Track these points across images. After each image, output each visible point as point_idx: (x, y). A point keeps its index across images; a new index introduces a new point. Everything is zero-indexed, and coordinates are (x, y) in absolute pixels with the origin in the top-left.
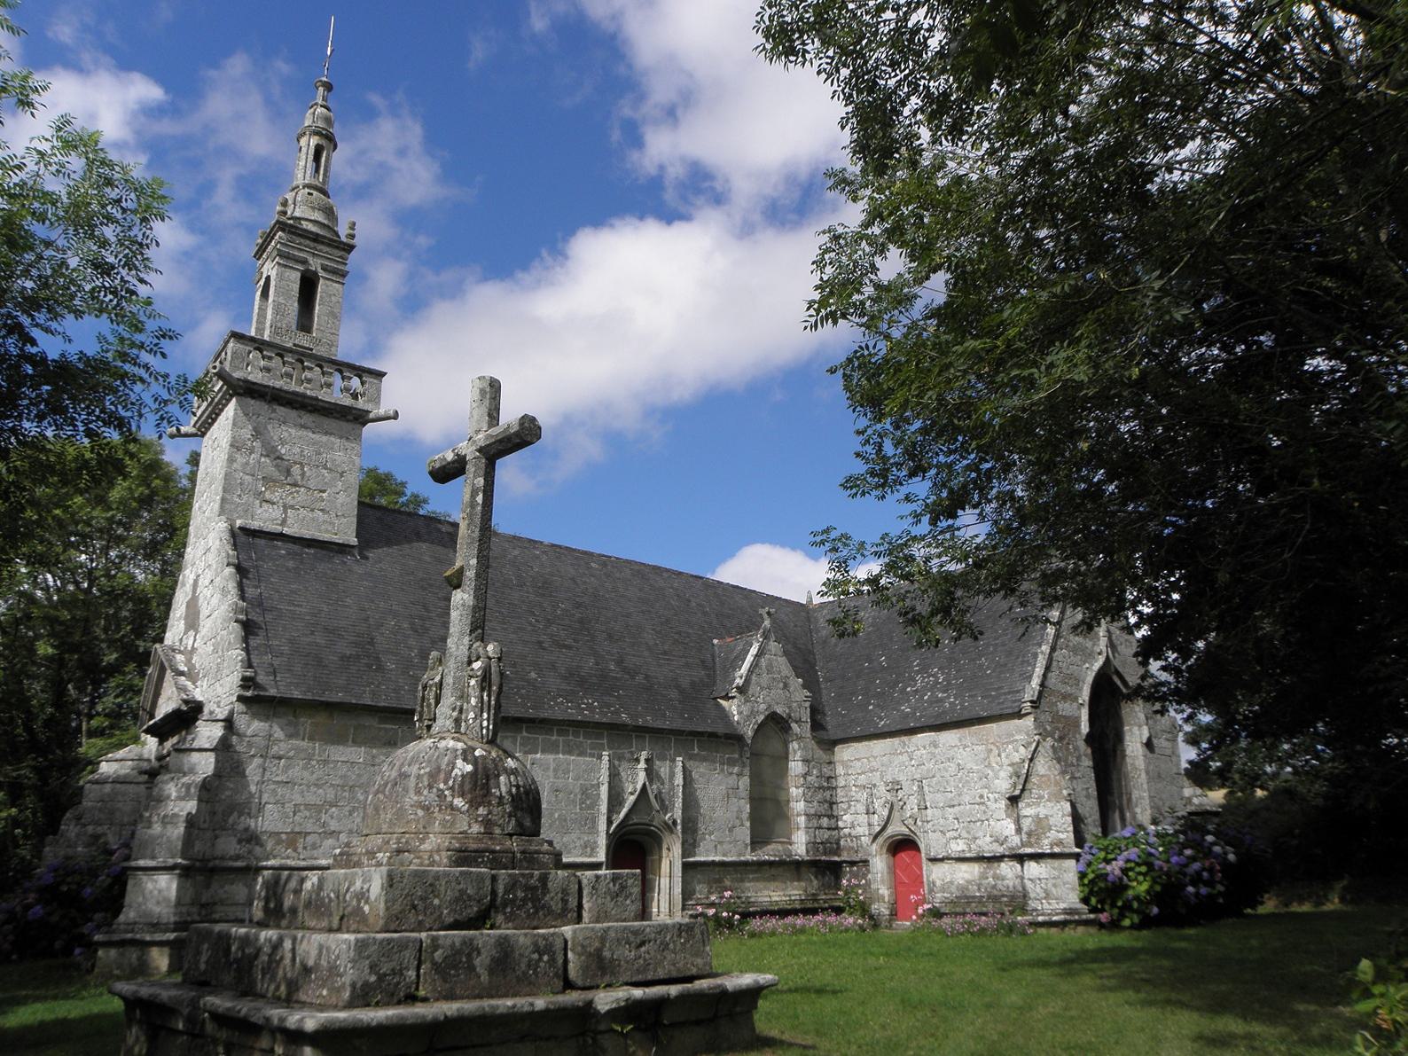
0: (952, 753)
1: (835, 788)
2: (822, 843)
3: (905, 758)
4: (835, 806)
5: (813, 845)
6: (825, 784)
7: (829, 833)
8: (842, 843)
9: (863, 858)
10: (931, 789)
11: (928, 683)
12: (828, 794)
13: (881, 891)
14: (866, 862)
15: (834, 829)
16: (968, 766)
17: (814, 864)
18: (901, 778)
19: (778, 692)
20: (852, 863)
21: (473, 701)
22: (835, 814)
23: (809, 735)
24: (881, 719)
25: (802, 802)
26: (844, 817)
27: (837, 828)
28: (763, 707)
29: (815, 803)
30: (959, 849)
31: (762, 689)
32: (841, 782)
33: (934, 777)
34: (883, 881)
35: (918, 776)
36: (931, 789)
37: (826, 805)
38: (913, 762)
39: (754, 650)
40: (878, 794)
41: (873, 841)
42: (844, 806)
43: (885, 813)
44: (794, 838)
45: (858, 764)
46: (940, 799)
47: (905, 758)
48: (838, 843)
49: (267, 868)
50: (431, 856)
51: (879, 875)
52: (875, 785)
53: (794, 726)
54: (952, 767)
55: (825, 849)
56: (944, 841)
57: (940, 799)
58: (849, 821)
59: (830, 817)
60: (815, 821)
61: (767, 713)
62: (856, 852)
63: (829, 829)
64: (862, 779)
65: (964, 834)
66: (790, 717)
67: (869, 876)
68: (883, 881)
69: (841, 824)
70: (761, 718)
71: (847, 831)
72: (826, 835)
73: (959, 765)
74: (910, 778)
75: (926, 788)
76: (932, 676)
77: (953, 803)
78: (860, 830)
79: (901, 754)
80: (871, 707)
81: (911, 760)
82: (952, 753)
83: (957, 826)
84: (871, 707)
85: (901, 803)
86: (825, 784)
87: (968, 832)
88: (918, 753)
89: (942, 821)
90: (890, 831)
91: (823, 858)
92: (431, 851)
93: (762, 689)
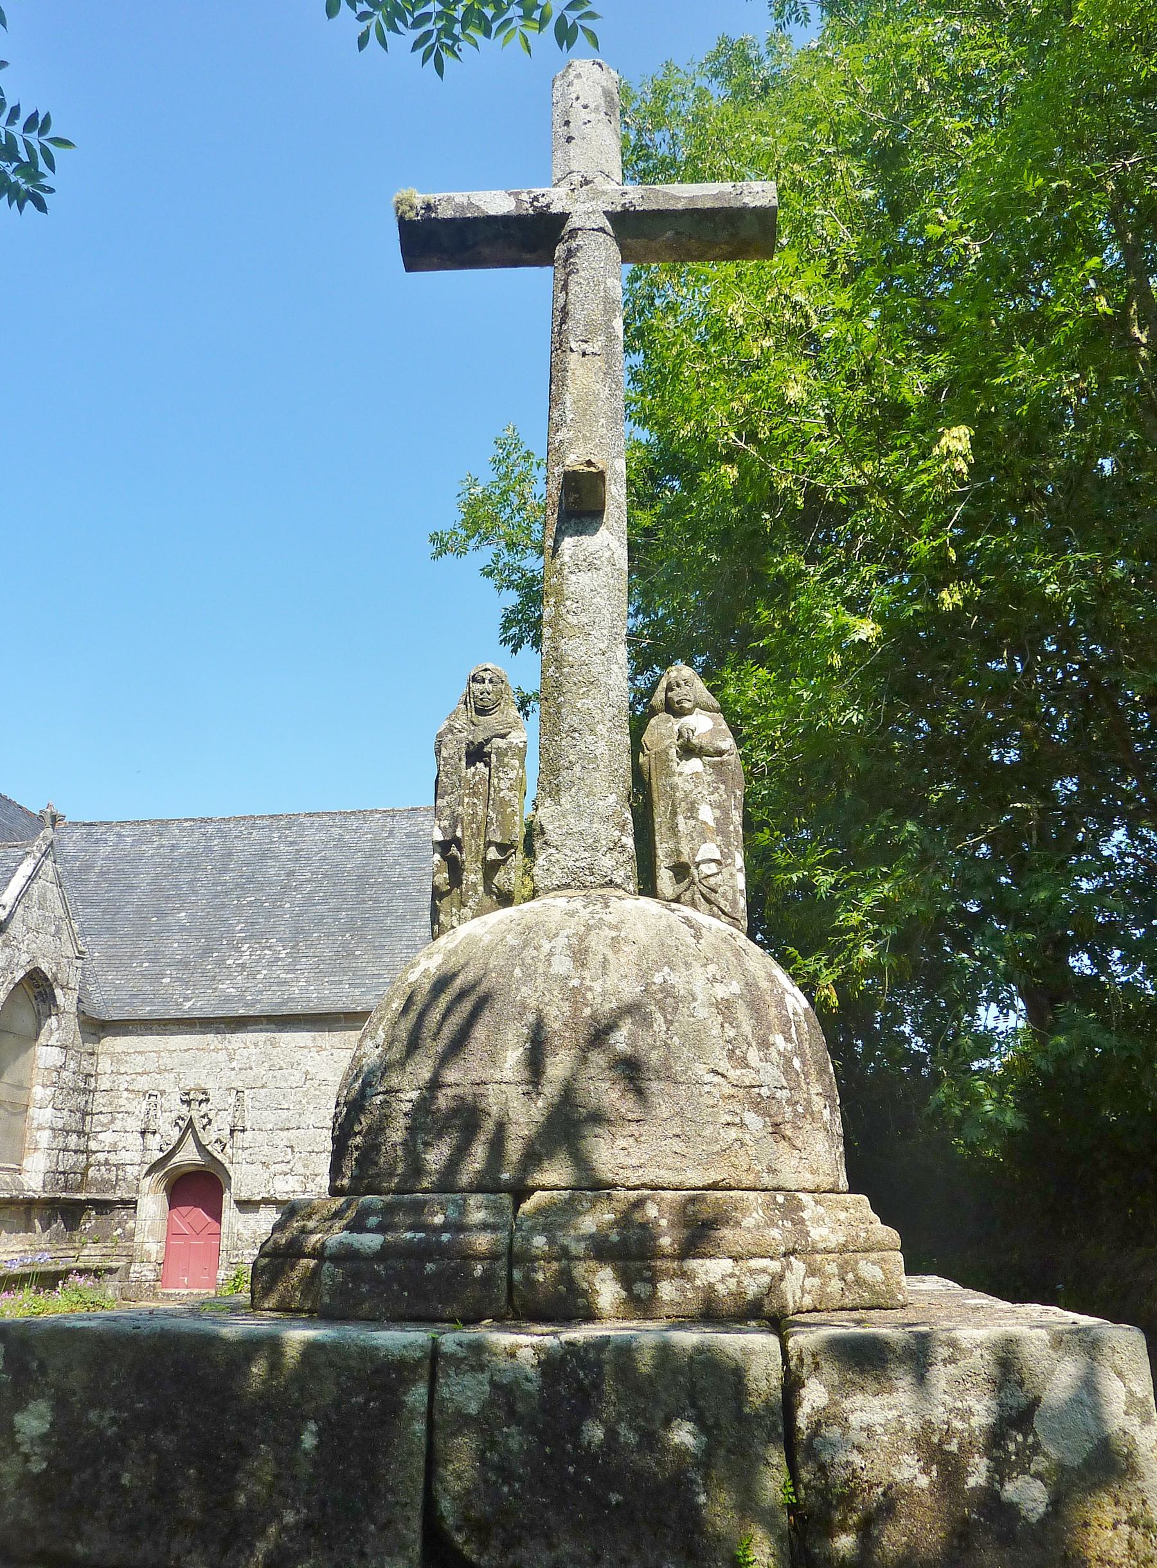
0: (298, 1056)
1: (94, 1091)
2: (63, 1173)
3: (222, 1056)
4: (88, 1118)
5: (56, 1175)
6: (82, 1084)
7: (75, 1157)
8: (92, 1172)
9: (126, 1196)
10: (257, 1104)
11: (261, 958)
12: (82, 1099)
13: (146, 1246)
14: (130, 1204)
15: (82, 1152)
16: (321, 1076)
17: (51, 1203)
18: (210, 1084)
19: (46, 939)
20: (103, 1207)
21: (706, 814)
22: (87, 1129)
23: (74, 1010)
24: (187, 999)
25: (50, 1110)
26: (101, 1136)
27: (88, 1152)
28: (25, 957)
29: (66, 1113)
30: (288, 1188)
31: (29, 930)
32: (104, 1083)
33: (263, 1087)
34: (151, 1232)
35: (238, 1084)
36: (257, 1104)
37: (78, 1115)
38: (234, 1064)
39: (26, 869)
40: (166, 1106)
41: (148, 1174)
42: (104, 1119)
43: (176, 1134)
44: (27, 1163)
45: (139, 1059)
46: (270, 1119)
47: (222, 1056)
48: (84, 1174)
49: (270, 1309)
50: (843, 1268)
51: (149, 1222)
52: (163, 1092)
53: (58, 992)
54: (296, 1077)
55: (66, 1181)
56: (266, 1176)
57: (270, 1119)
58: (108, 1141)
59: (81, 1133)
60: (61, 1139)
61: (28, 968)
62: (114, 1187)
63: (76, 1152)
64: (143, 1083)
65: (299, 1169)
66: (56, 980)
67: (131, 1224)
68: (151, 1232)
69: (93, 1145)
70: (20, 974)
71: (101, 1157)
72: (70, 1160)
73: (307, 1073)
74: (224, 1086)
75: (248, 1102)
76: (269, 948)
77: (288, 1125)
78: (124, 1156)
79: (216, 1050)
80: (166, 980)
81: (231, 1060)
82: (298, 1056)
83: (289, 1157)
84: (166, 980)
85: (205, 1121)
86: (82, 1084)
87: (305, 1166)
88: (245, 1052)
89: (266, 1149)
90: (177, 1159)
91: (64, 1195)
92: (843, 1249)
93: (29, 930)
